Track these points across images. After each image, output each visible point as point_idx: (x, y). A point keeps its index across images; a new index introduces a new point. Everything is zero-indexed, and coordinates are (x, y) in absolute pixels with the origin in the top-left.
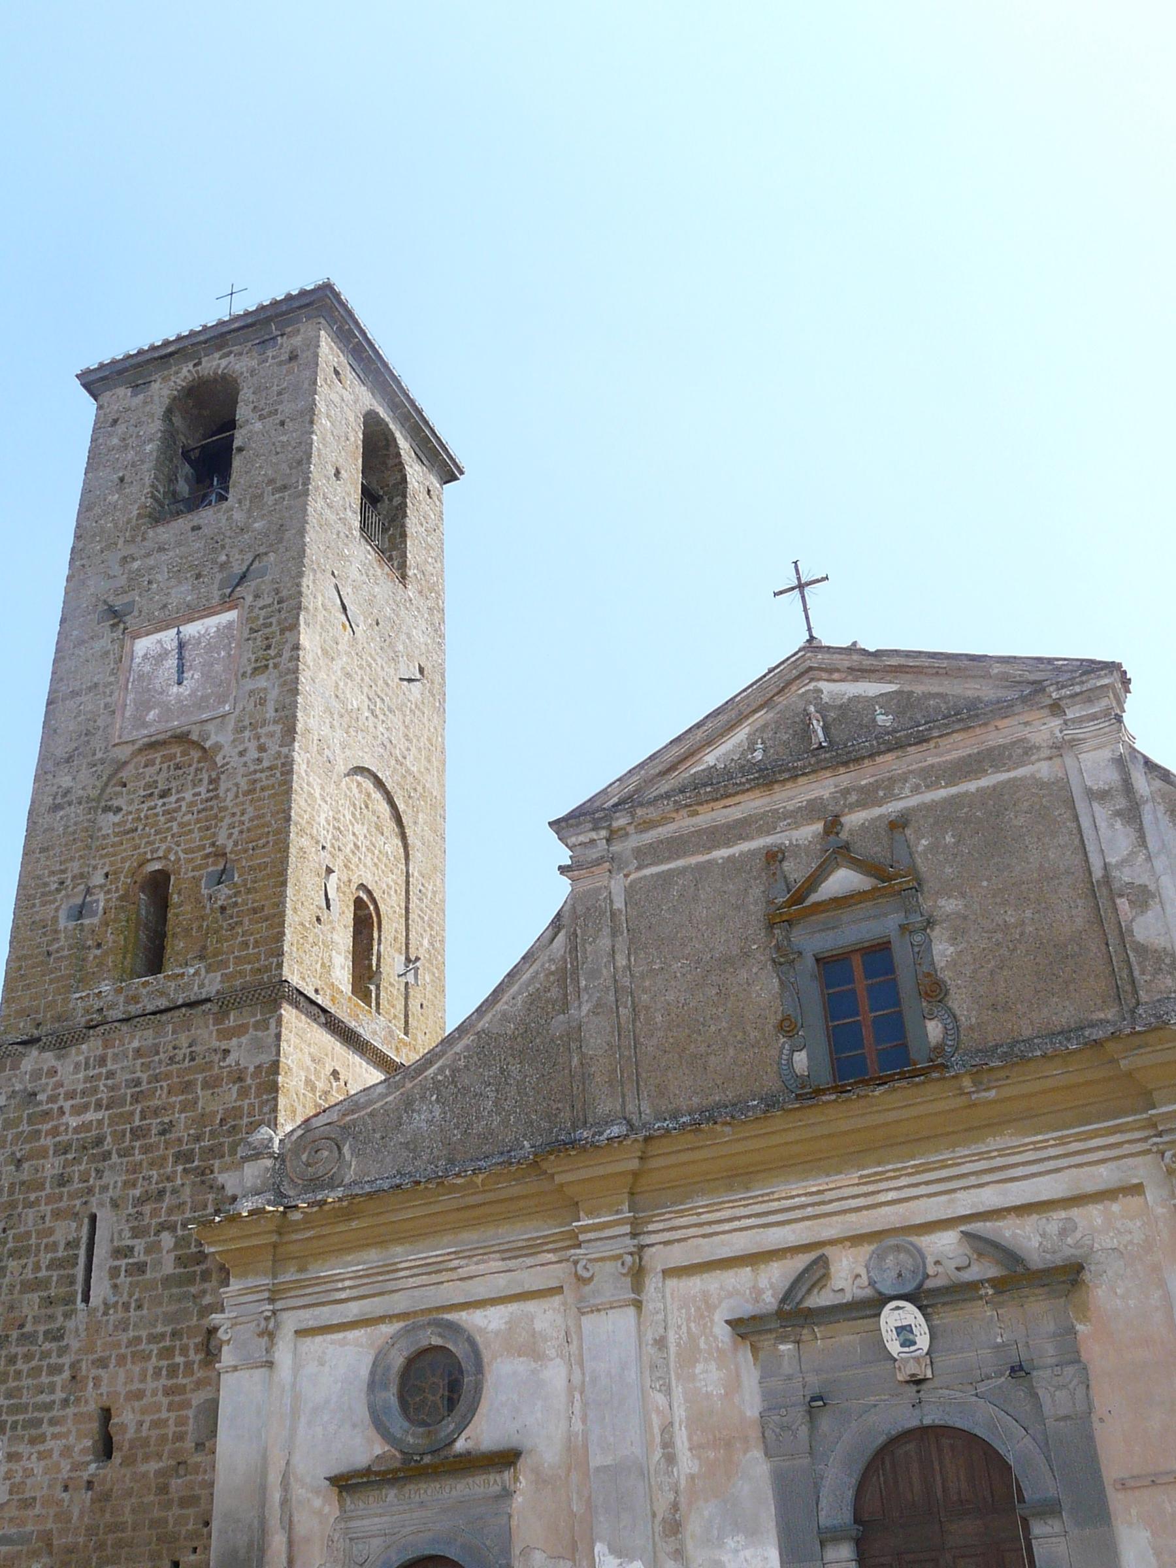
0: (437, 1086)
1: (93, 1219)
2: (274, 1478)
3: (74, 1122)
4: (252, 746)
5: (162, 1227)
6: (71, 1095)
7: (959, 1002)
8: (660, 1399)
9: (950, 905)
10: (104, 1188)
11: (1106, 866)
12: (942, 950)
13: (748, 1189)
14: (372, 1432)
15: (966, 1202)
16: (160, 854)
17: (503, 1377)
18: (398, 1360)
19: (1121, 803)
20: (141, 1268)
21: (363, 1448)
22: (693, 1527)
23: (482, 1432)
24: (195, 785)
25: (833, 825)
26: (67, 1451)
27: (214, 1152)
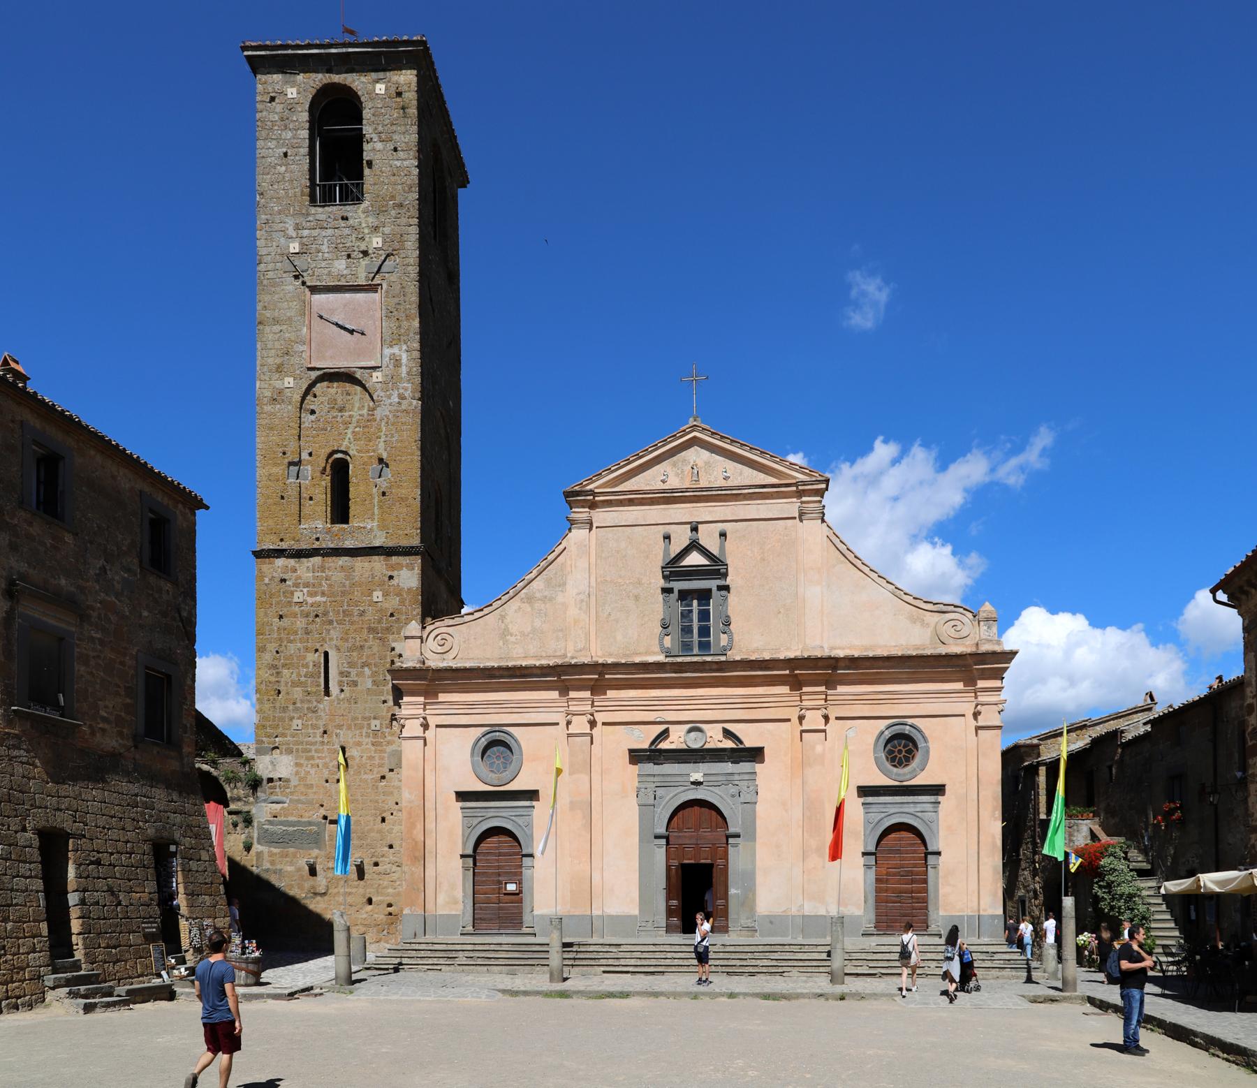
1: (326, 654)
3: (310, 600)
4: (396, 393)
5: (364, 665)
6: (307, 585)
10: (331, 639)
16: (343, 448)
20: (355, 684)
24: (359, 409)
26: (326, 766)
27: (388, 630)
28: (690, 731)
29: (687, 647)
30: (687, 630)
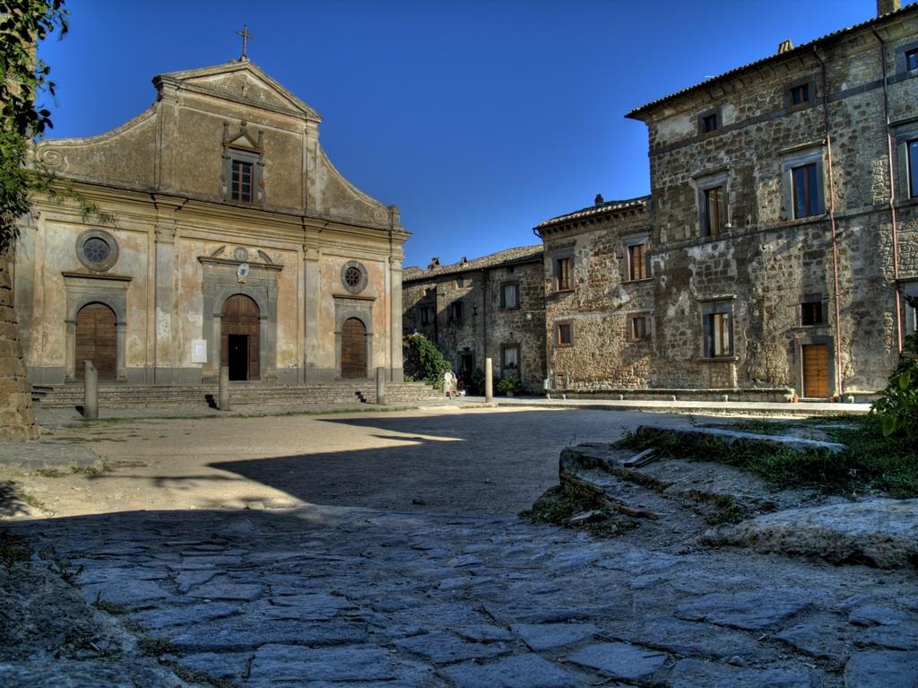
0: (103, 149)
2: (38, 267)
7: (267, 189)
8: (176, 271)
9: (269, 162)
11: (307, 171)
12: (265, 174)
13: (206, 220)
14: (77, 260)
15: (261, 243)
17: (125, 252)
18: (85, 238)
19: (313, 155)
21: (74, 266)
22: (181, 307)
23: (117, 270)
25: (243, 124)
28: (237, 249)
29: (235, 196)
30: (235, 187)
